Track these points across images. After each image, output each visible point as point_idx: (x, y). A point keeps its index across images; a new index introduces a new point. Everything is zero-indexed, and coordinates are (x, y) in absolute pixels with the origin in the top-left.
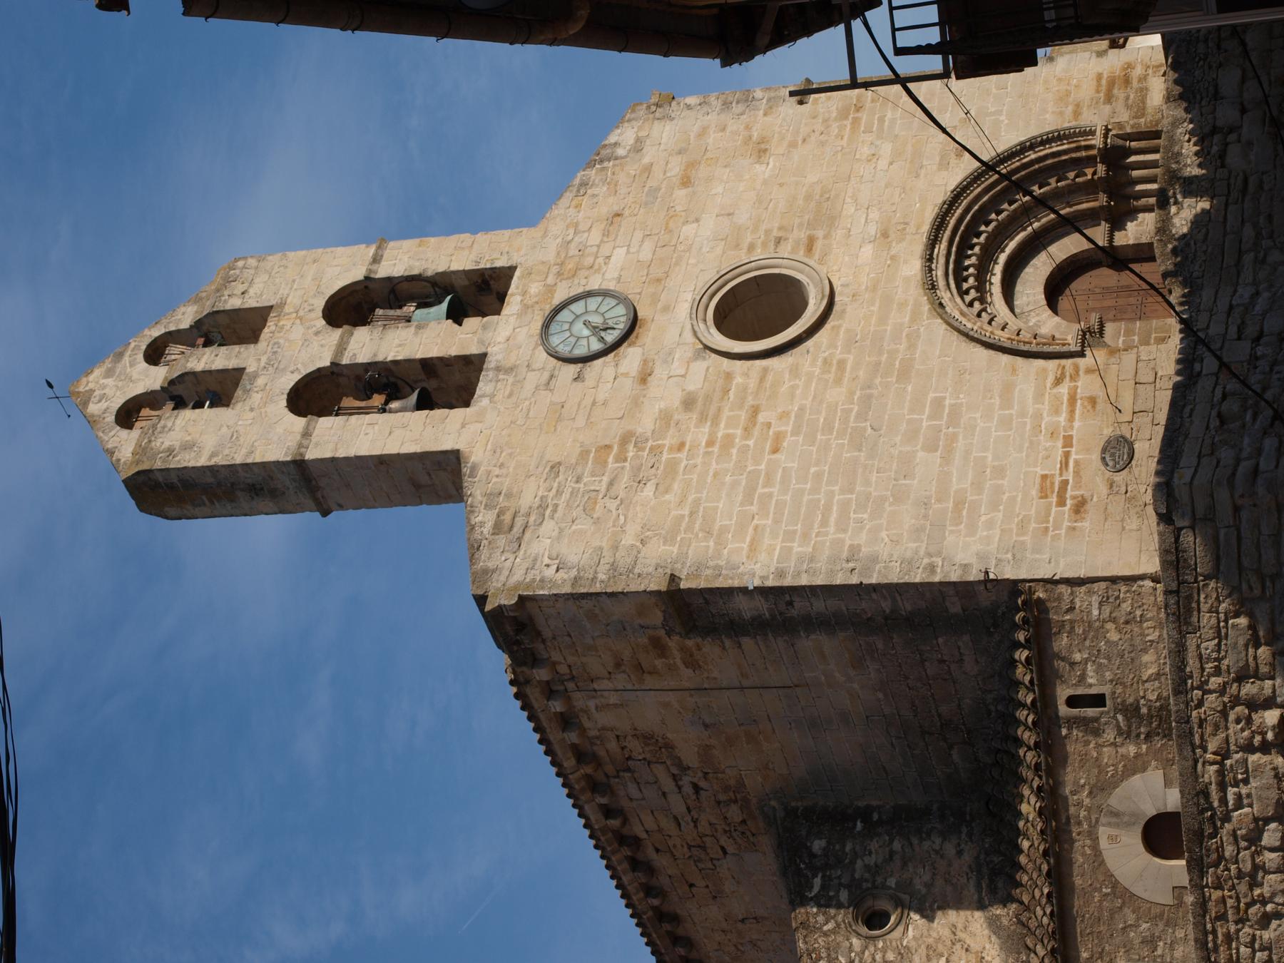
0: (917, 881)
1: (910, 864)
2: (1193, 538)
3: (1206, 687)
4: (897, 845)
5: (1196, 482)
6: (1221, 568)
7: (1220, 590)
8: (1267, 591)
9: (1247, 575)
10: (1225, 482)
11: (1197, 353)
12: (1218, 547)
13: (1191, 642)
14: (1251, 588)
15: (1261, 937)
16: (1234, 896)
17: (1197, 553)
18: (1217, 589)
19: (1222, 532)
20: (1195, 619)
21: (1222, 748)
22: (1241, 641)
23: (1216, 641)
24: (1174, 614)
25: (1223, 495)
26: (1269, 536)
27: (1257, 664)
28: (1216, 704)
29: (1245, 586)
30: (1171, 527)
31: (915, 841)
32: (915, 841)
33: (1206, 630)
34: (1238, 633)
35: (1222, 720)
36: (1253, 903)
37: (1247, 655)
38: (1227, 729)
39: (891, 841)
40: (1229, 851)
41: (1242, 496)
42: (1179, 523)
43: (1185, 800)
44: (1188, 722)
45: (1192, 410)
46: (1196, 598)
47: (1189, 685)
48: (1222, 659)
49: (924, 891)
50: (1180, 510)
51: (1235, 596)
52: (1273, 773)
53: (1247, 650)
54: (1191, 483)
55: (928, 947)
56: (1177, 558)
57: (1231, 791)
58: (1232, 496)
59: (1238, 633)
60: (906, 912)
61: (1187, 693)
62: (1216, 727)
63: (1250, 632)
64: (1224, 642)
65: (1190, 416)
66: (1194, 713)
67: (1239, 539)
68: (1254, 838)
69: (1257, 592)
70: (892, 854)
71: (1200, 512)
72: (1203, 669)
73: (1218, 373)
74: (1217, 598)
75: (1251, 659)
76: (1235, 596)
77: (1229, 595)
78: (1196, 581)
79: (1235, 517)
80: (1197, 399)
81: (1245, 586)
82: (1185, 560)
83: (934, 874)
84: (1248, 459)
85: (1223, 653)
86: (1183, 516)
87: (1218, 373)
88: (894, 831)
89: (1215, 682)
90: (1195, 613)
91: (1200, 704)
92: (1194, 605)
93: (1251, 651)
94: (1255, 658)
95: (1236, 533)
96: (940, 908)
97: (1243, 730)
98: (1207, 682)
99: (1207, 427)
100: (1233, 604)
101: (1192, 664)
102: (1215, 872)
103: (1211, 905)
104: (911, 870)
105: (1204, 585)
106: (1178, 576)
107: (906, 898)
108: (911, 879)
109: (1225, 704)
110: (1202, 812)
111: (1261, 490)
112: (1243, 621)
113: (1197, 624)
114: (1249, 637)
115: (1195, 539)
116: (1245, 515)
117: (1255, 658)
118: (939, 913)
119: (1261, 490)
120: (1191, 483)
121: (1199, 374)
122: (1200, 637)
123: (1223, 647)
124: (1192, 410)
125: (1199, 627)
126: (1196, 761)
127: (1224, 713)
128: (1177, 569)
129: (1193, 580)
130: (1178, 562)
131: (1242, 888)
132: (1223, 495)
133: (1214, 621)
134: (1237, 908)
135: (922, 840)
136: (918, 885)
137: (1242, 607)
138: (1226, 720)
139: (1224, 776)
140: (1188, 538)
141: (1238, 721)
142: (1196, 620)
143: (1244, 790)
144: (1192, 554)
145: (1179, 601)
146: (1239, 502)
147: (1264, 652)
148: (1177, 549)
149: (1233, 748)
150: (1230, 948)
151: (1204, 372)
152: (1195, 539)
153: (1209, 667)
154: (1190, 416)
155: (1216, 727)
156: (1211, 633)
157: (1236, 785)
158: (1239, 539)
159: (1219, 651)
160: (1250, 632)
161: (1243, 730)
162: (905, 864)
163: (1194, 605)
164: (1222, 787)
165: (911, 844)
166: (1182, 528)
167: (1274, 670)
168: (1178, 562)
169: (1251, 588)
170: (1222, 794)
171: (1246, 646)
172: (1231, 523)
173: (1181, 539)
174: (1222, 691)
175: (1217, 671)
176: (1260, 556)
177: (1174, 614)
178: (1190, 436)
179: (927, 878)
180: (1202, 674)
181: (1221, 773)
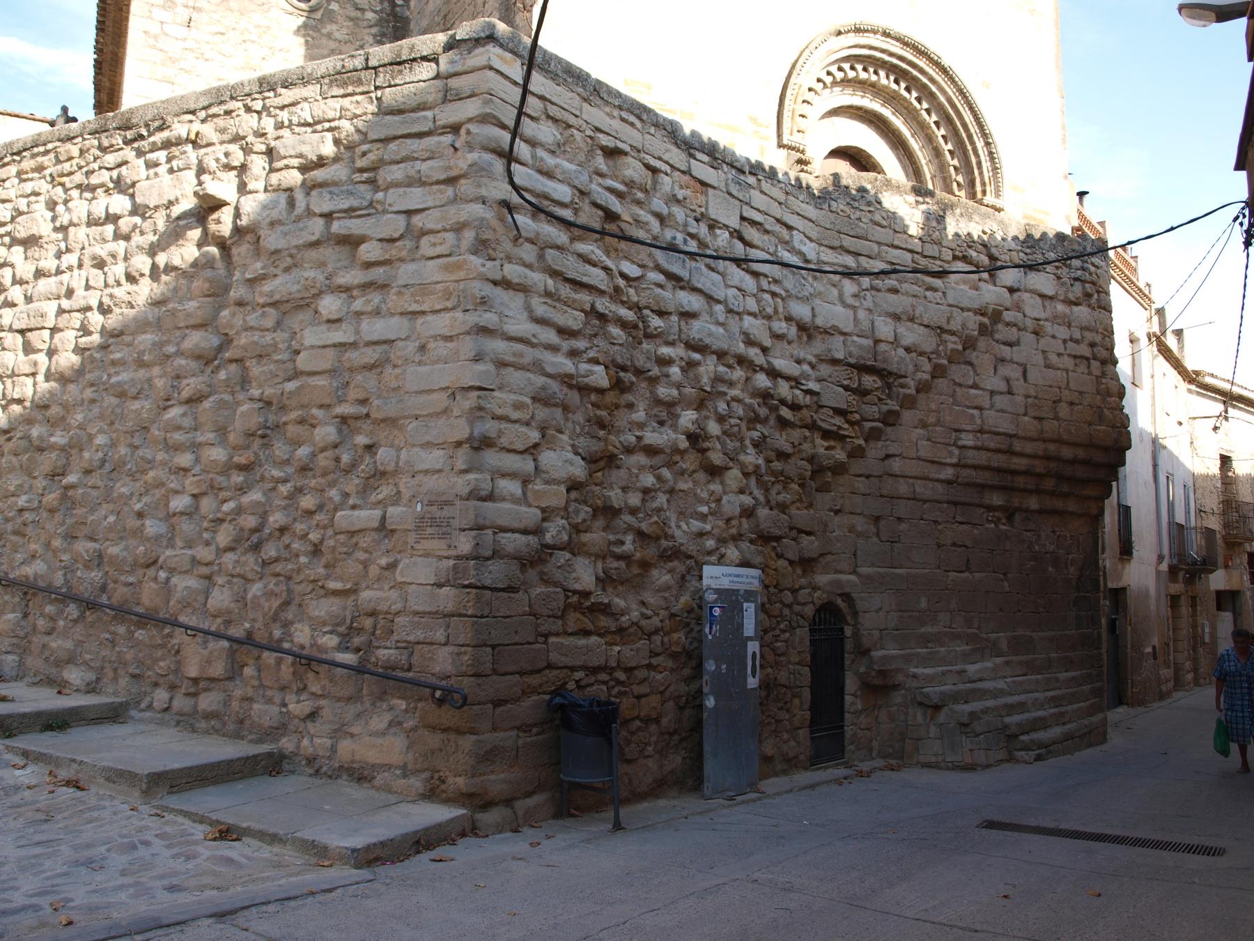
0: (334, 27)
1: (351, 23)
2: (425, 78)
3: (264, 114)
4: (370, 15)
5: (491, 74)
6: (388, 117)
7: (364, 118)
8: (357, 175)
9: (378, 149)
10: (488, 111)
11: (724, 166)
12: (413, 110)
13: (312, 91)
14: (364, 154)
15: (37, 202)
16: (72, 170)
17: (407, 86)
18: (365, 114)
19: (429, 114)
20: (337, 91)
21: (202, 140)
22: (306, 149)
23: (311, 121)
24: (343, 67)
25: (471, 108)
26: (419, 172)
27: (281, 169)
28: (245, 128)
29: (365, 147)
30: (440, 50)
31: (374, 30)
32: (374, 30)
33: (323, 106)
34: (315, 144)
35: (230, 136)
36: (66, 190)
37: (291, 156)
38: (222, 143)
39: (375, 12)
40: (110, 159)
41: (468, 132)
42: (443, 60)
43: (158, 105)
44: (232, 98)
45: (632, 124)
46: (358, 90)
47: (267, 94)
48: (291, 130)
49: (324, 31)
50: (458, 57)
51: (356, 137)
52: (172, 198)
53: (297, 157)
54: (491, 68)
55: (268, 28)
56: (404, 62)
57: (161, 155)
58: (470, 120)
59: (315, 144)
60: (305, 14)
61: (260, 93)
62: (222, 131)
63: (315, 159)
64: (309, 129)
65: (623, 120)
66: (240, 104)
67: (420, 135)
68: (121, 186)
69: (360, 163)
70: (362, 10)
71: (454, 83)
72: (282, 108)
73: (691, 175)
74: (356, 116)
75: (285, 162)
76: (356, 137)
77: (358, 131)
78: (377, 88)
79: (444, 127)
80: (649, 137)
81: (365, 147)
82: (400, 72)
83: (340, 42)
84: (534, 156)
85: (297, 129)
86: (452, 62)
87: (691, 175)
88: (384, 15)
89: (268, 124)
90: (341, 92)
91: (248, 109)
92: (350, 89)
93: (295, 162)
94: (287, 167)
95: (426, 129)
96: (307, 42)
97: (217, 160)
98: (269, 115)
99: (598, 130)
100: (348, 136)
101: (287, 95)
102: (93, 147)
103: (68, 146)
104: (346, 24)
105: (371, 98)
106: (384, 65)
107: (318, 15)
108: (336, 23)
109: (244, 138)
110: (147, 126)
111: (473, 156)
112: (328, 149)
113: (329, 95)
114: (309, 157)
115: (424, 81)
116: (448, 139)
117: (287, 167)
118: (302, 40)
119: (473, 156)
120: (491, 68)
121: (692, 156)
122: (316, 100)
123: (304, 129)
124: (632, 124)
125: (326, 98)
126: (193, 112)
127: (237, 138)
128: (391, 64)
129: (377, 84)
130: (399, 63)
131: (79, 178)
132: (471, 108)
133: (331, 115)
134: (62, 175)
135: (375, 36)
136: (330, 28)
137: (345, 148)
138: (230, 142)
139: (177, 144)
140: (426, 71)
141: (227, 155)
142: (334, 94)
143: (162, 170)
144: (408, 80)
145: (357, 71)
146: (463, 131)
147: (294, 177)
148: (414, 60)
149: (202, 151)
150: (33, 170)
151: (692, 161)
152: (424, 81)
153: (284, 116)
154: (623, 120)
155: (222, 131)
156: (318, 113)
157: (169, 160)
158: (420, 135)
159: (300, 125)
160: (315, 159)
161: (217, 160)
162: (351, 19)
163: (350, 89)
164: (167, 145)
165: (371, 27)
166: (437, 64)
167: (274, 191)
168: (399, 63)
169: (364, 154)
170: (160, 145)
171: (301, 156)
172: (438, 123)
173: (425, 64)
174: (261, 134)
175: (279, 126)
176: (398, 163)
177: (343, 67)
178: (585, 105)
179: (337, 35)
180: (278, 108)
181: (179, 142)
